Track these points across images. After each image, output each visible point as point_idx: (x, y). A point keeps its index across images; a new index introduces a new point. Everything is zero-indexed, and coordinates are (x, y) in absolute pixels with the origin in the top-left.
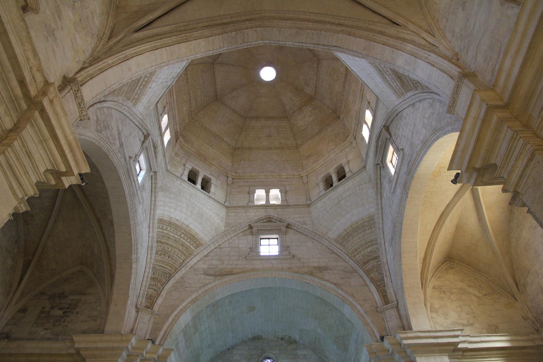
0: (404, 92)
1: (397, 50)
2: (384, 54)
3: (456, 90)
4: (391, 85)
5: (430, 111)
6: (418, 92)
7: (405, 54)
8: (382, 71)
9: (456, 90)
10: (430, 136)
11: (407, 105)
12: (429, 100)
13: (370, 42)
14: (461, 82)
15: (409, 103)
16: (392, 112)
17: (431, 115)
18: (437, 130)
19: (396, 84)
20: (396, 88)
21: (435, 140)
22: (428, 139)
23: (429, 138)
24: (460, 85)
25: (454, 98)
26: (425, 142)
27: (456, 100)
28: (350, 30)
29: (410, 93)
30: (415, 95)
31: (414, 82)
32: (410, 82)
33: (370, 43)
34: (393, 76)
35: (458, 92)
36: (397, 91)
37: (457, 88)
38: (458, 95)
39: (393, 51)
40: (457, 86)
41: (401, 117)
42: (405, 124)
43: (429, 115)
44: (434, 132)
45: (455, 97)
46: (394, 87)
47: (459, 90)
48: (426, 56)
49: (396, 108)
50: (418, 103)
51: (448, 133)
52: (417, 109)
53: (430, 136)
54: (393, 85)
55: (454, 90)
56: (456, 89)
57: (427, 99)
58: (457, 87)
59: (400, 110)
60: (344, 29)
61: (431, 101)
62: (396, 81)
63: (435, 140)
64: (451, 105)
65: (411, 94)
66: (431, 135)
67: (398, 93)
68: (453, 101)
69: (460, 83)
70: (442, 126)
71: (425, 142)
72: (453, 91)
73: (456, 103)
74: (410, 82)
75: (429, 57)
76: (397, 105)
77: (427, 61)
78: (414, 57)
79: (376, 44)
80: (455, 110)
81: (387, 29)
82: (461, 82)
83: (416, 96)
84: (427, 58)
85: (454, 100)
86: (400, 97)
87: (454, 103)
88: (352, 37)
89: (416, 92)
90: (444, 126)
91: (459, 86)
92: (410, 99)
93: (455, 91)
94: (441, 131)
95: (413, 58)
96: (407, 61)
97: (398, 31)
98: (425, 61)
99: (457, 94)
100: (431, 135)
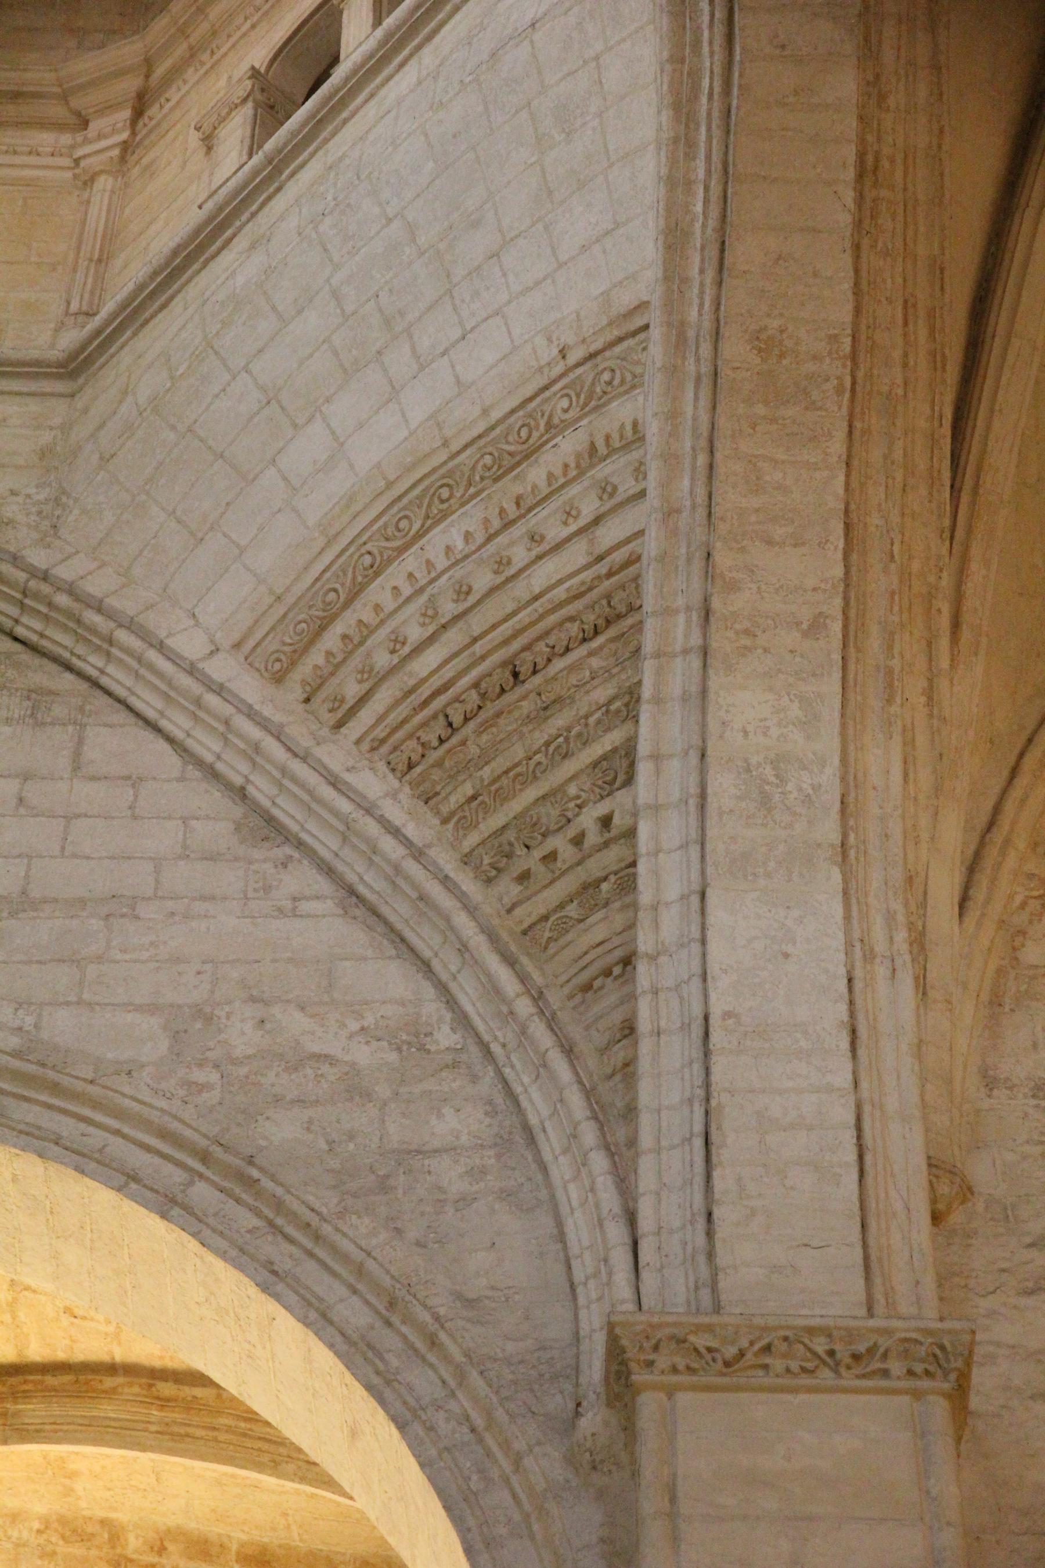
0: (366, 717)
1: (837, 657)
2: (770, 542)
3: (831, 1353)
4: (376, 571)
5: (363, 1054)
6: (469, 884)
7: (829, 743)
8: (511, 488)
9: (831, 1353)
10: (147, 1125)
11: (236, 769)
12: (432, 1007)
13: (839, 391)
14: (910, 1373)
15: (257, 779)
16: (62, 600)
17: (331, 1073)
18: (250, 1183)
19: (415, 633)
20: (367, 630)
21: (135, 1178)
22: (96, 1105)
23: (120, 1114)
24: (885, 1373)
25: (768, 1349)
26: (55, 1088)
27: (760, 1378)
28: (892, 161)
29: (394, 795)
30: (418, 854)
31: (558, 842)
32: (532, 793)
33: (829, 386)
34: (505, 603)
35: (826, 1375)
36: (331, 640)
37: (856, 1357)
38: (805, 1380)
39: (816, 627)
40: (871, 1351)
41: (59, 711)
42: (26, 777)
43: (316, 1048)
44: (205, 1157)
45: (778, 1364)
46: (362, 611)
47: (848, 1380)
48: (880, 946)
49: (122, 636)
50: (322, 885)
51: (293, 1298)
52: (267, 889)
53: (147, 1125)
54: (379, 592)
55: (827, 1332)
56: (843, 1353)
57: (429, 991)
58: (861, 1348)
59: (117, 678)
60: (891, 101)
61: (446, 1037)
62: (454, 637)
63: (135, 1178)
64: (700, 1341)
65: (395, 814)
66: (163, 1134)
67: (316, 657)
68: (742, 1354)
69: (896, 1367)
70: (327, 1229)
71: (55, 1088)
72: (811, 1331)
73: (738, 1389)
74: (532, 793)
75: (882, 971)
76: (161, 647)
77: (858, 973)
78: (835, 838)
79: (837, 446)
80: (671, 1392)
81: (923, 491)
82: (910, 1373)
83: (412, 867)
84: (869, 957)
85: (749, 1356)
86: (279, 679)
87: (727, 1364)
88: (849, 196)
89: (446, 861)
90: (345, 1258)
91: (877, 1365)
92: (345, 806)
93: (820, 1346)
94: (256, 1222)
95: (829, 830)
96: (782, 780)
97: (929, 597)
98: (849, 945)
99: (804, 1370)
100: (163, 1134)
